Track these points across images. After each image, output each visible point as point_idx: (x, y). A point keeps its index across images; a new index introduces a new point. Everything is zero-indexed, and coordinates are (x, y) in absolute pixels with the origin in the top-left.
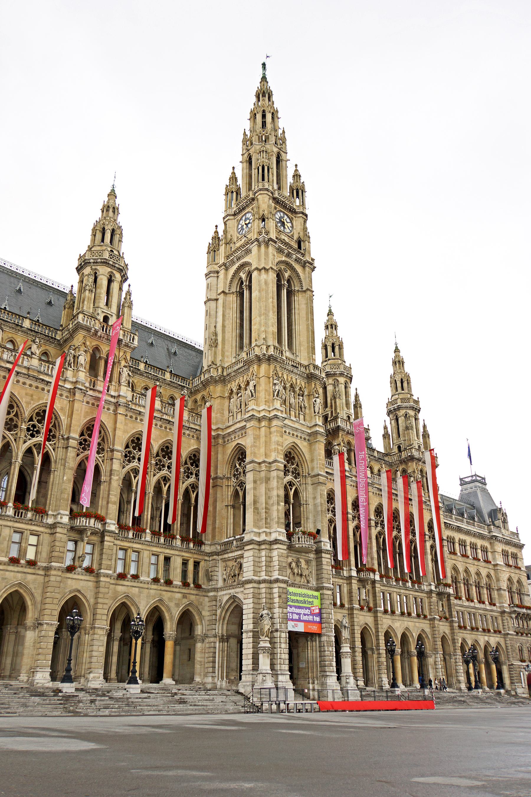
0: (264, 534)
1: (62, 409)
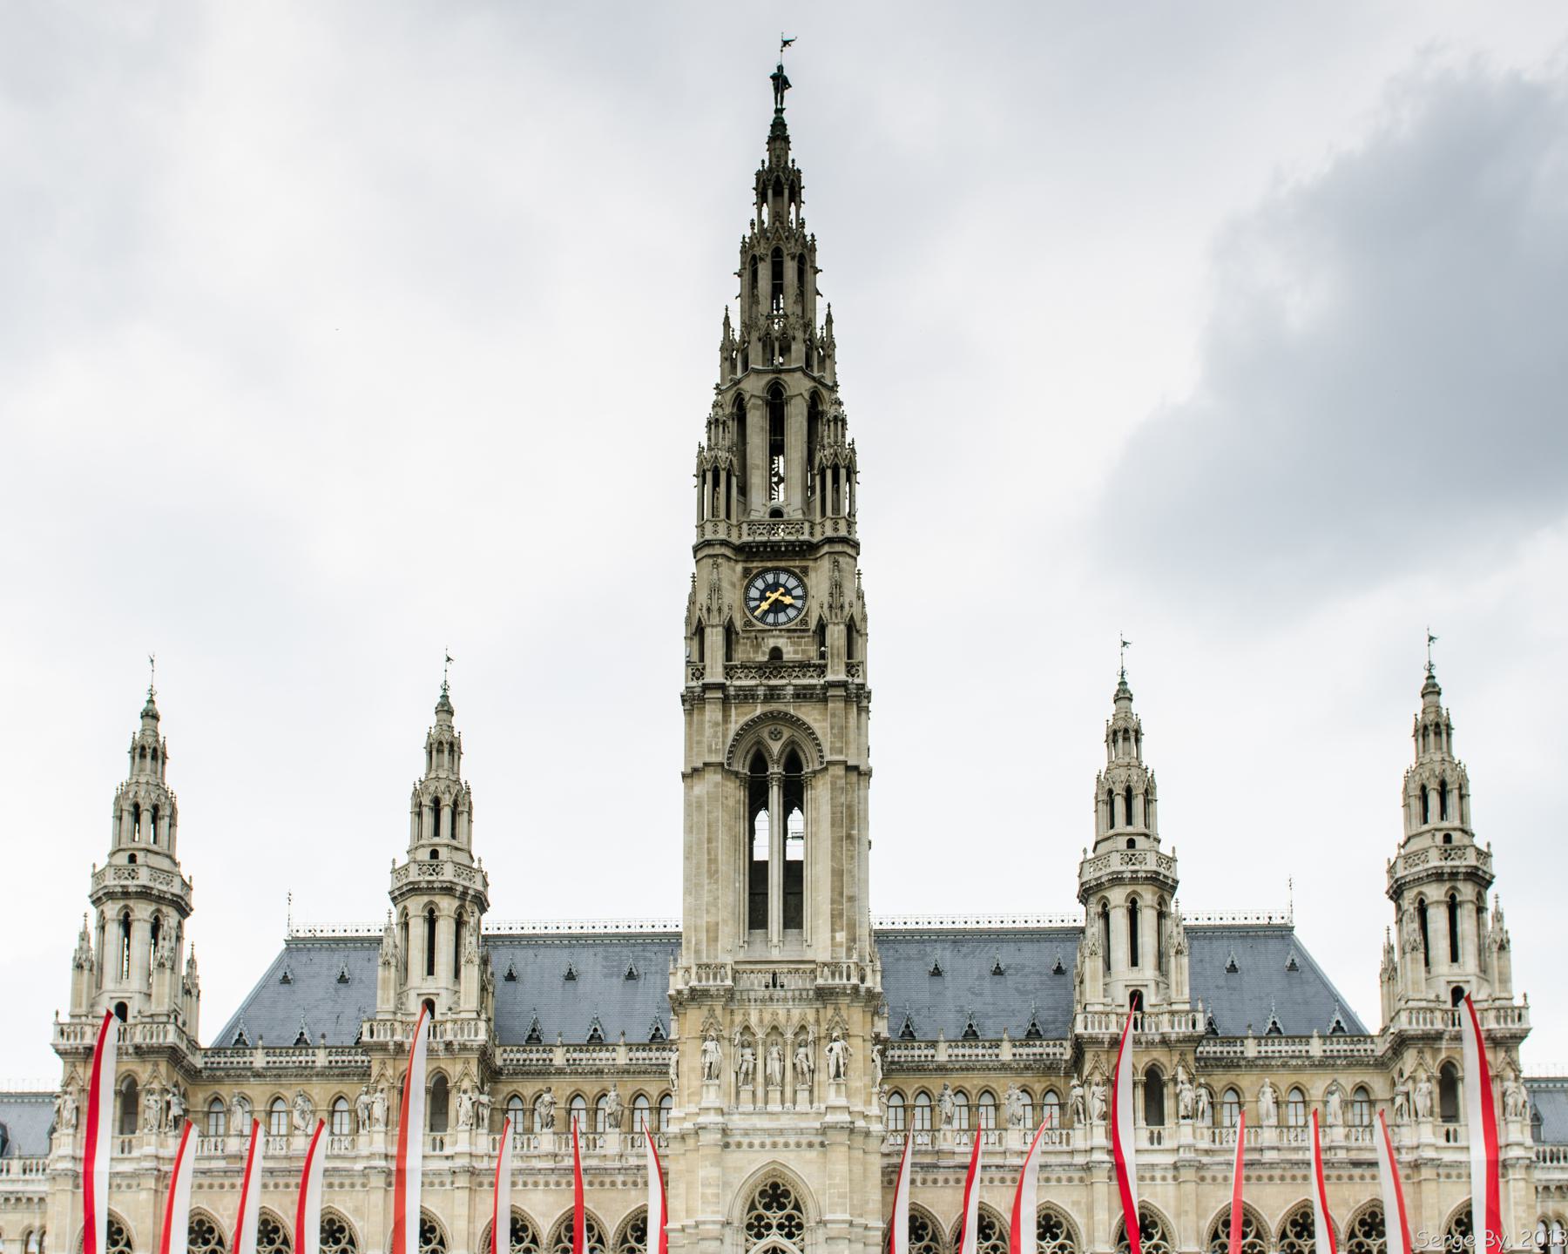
1: (357, 1210)
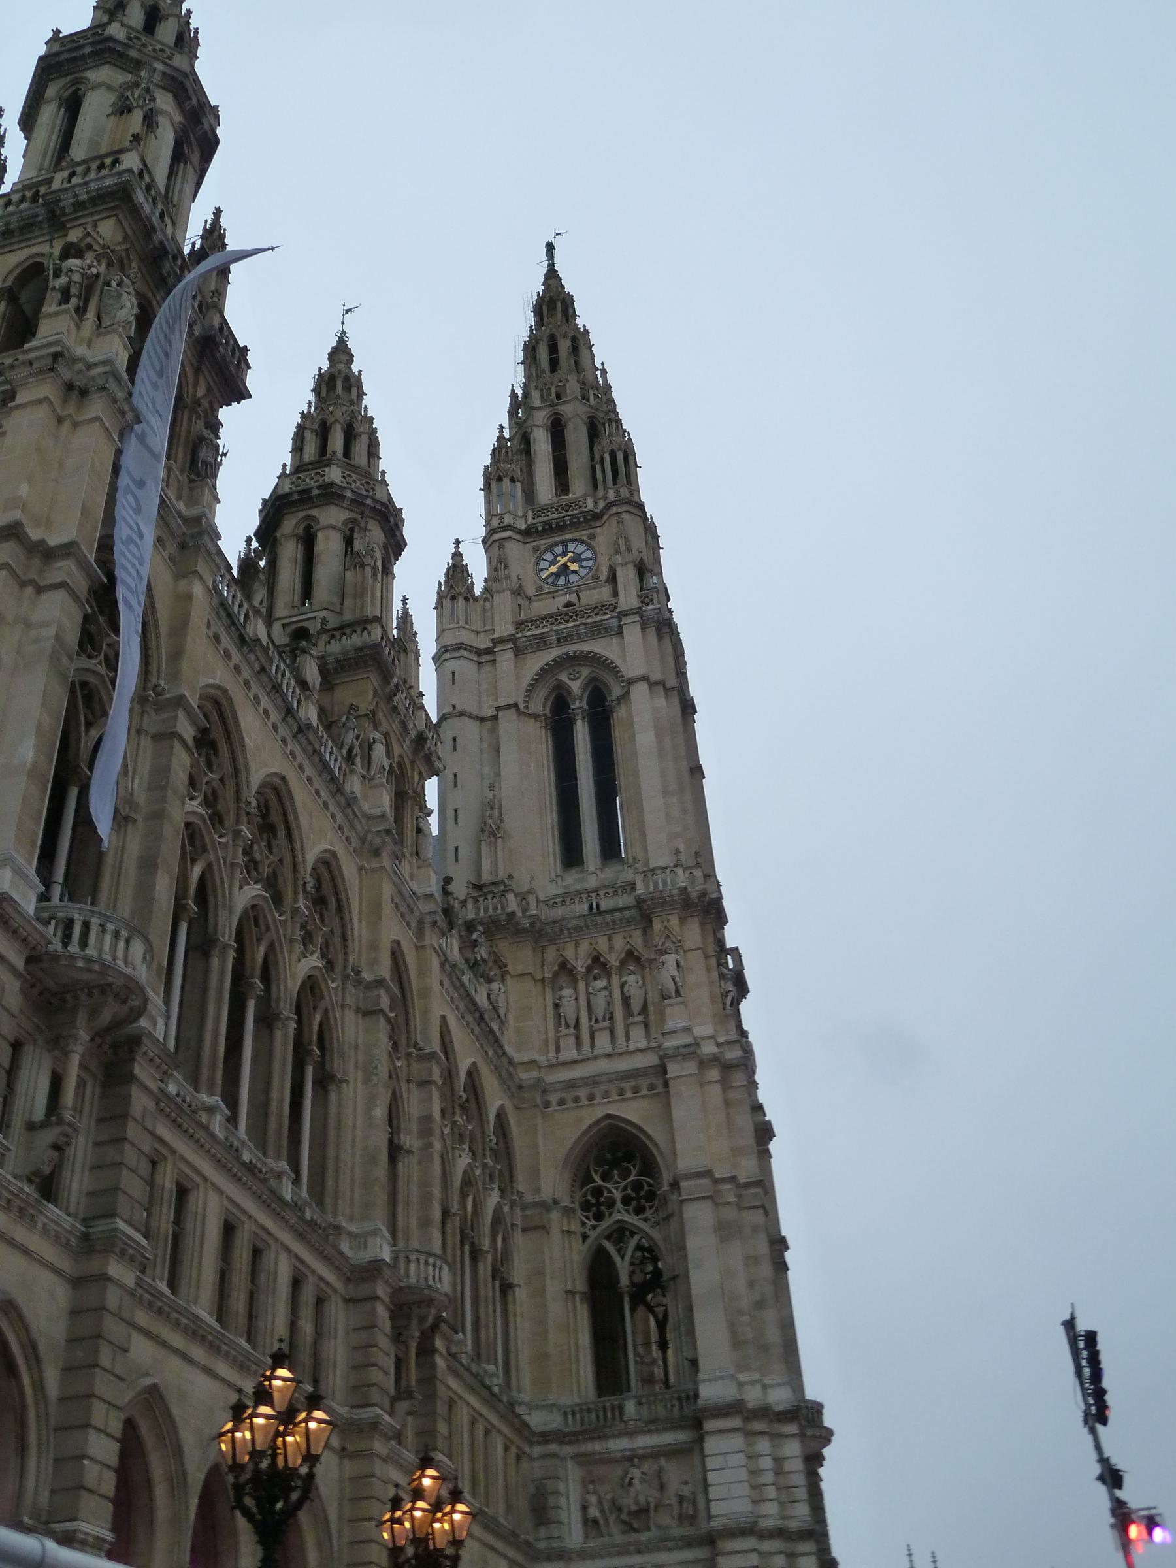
0: (758, 1387)
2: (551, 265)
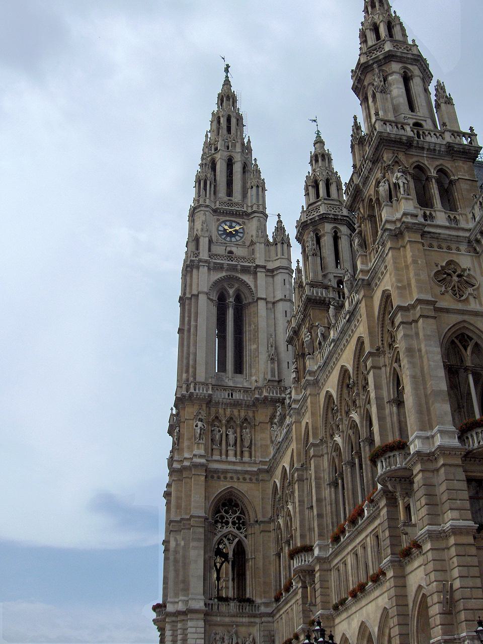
2: (227, 77)
